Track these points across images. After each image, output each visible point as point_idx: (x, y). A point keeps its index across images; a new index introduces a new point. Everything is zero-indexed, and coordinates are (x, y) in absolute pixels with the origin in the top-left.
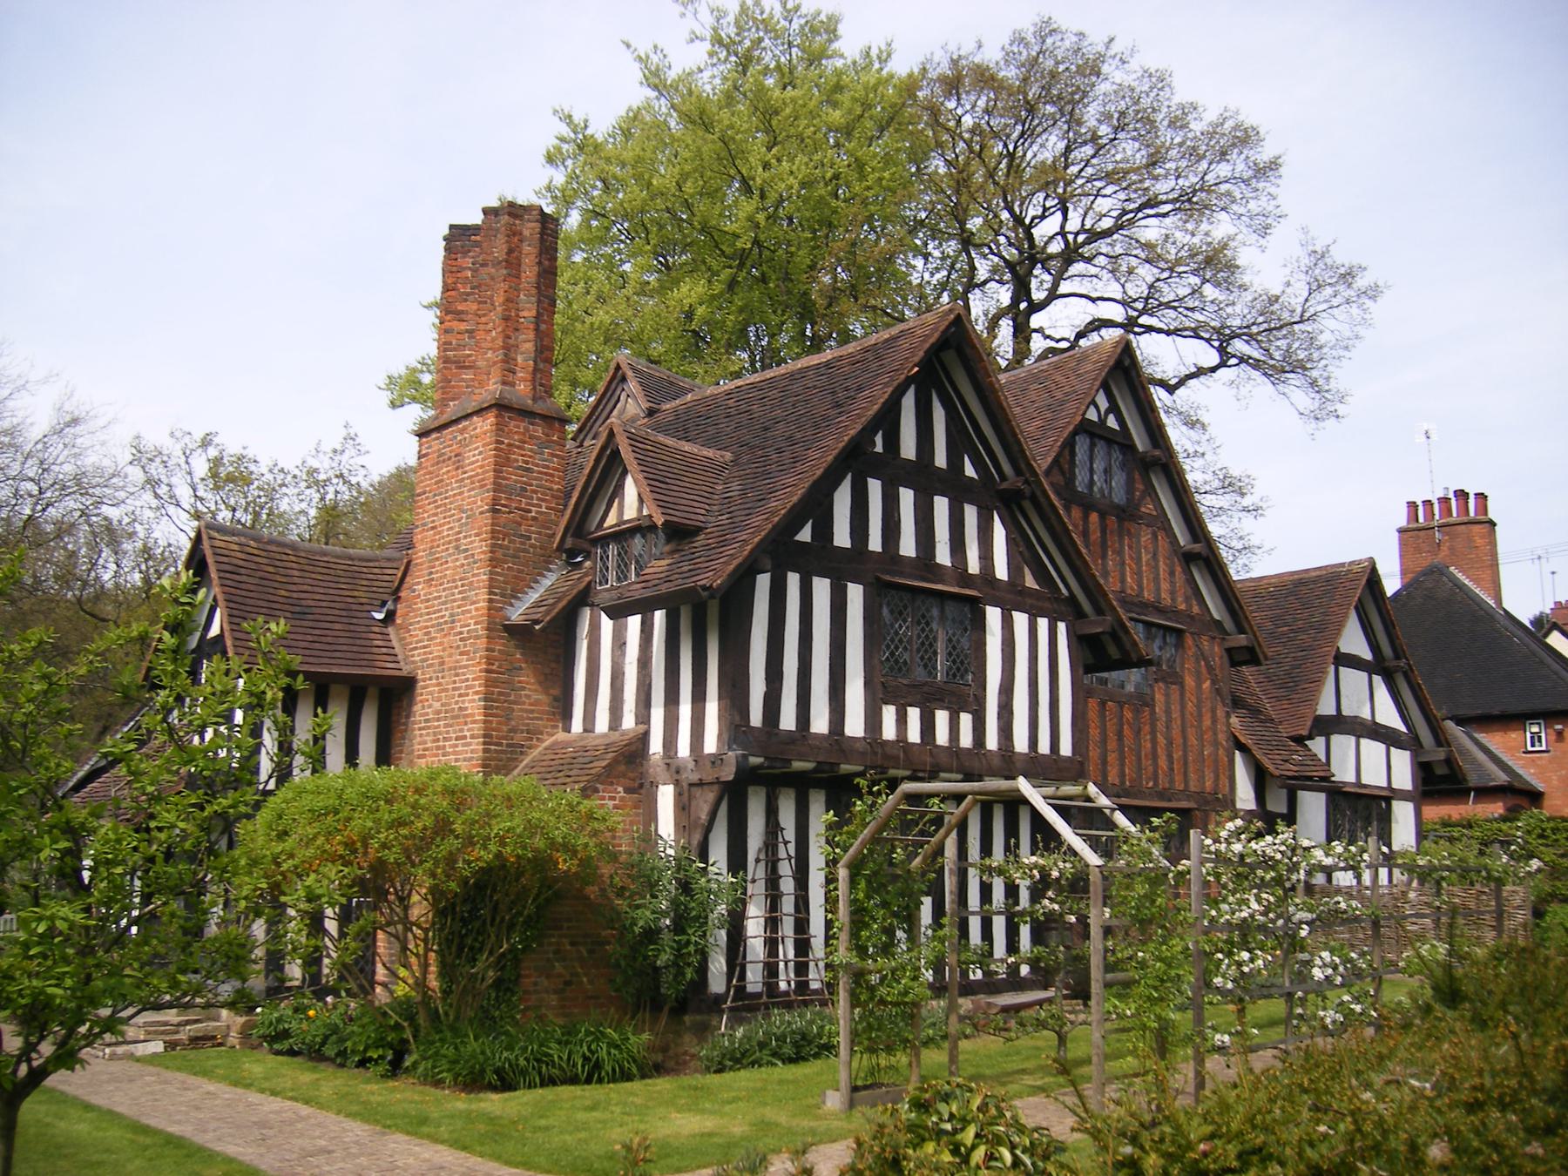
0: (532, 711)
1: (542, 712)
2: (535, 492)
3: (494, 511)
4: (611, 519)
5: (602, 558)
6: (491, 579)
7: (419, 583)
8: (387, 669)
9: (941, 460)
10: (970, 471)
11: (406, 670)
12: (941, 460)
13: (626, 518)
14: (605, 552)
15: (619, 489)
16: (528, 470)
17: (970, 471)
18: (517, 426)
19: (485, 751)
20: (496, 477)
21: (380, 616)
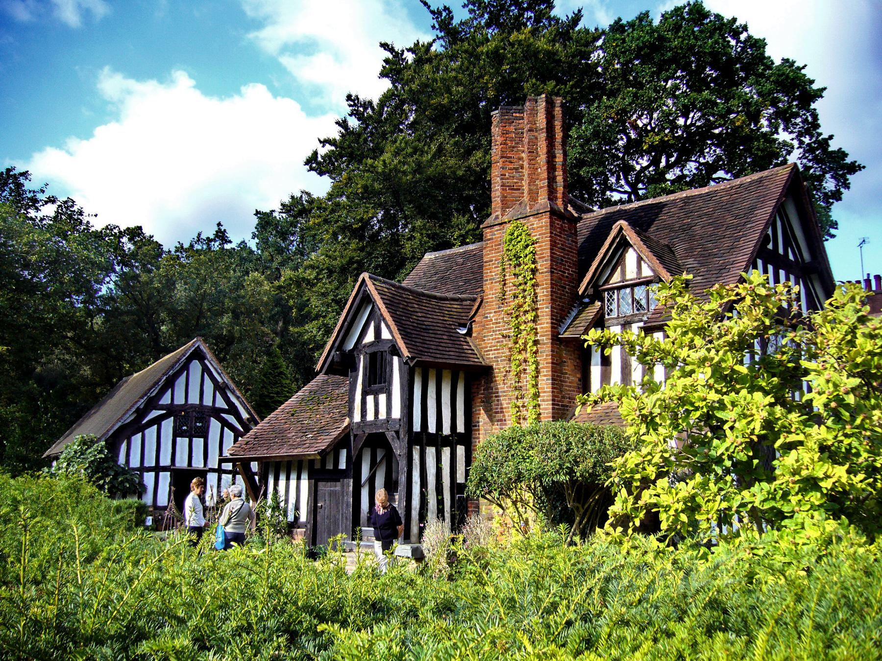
0: (570, 387)
1: (574, 387)
2: (566, 262)
3: (552, 272)
4: (616, 278)
5: (608, 300)
6: (552, 311)
7: (490, 313)
8: (473, 361)
9: (781, 251)
10: (791, 257)
11: (487, 362)
12: (781, 251)
13: (628, 277)
14: (611, 297)
15: (621, 261)
16: (563, 249)
17: (791, 257)
18: (558, 223)
19: (553, 409)
20: (551, 253)
21: (464, 331)
